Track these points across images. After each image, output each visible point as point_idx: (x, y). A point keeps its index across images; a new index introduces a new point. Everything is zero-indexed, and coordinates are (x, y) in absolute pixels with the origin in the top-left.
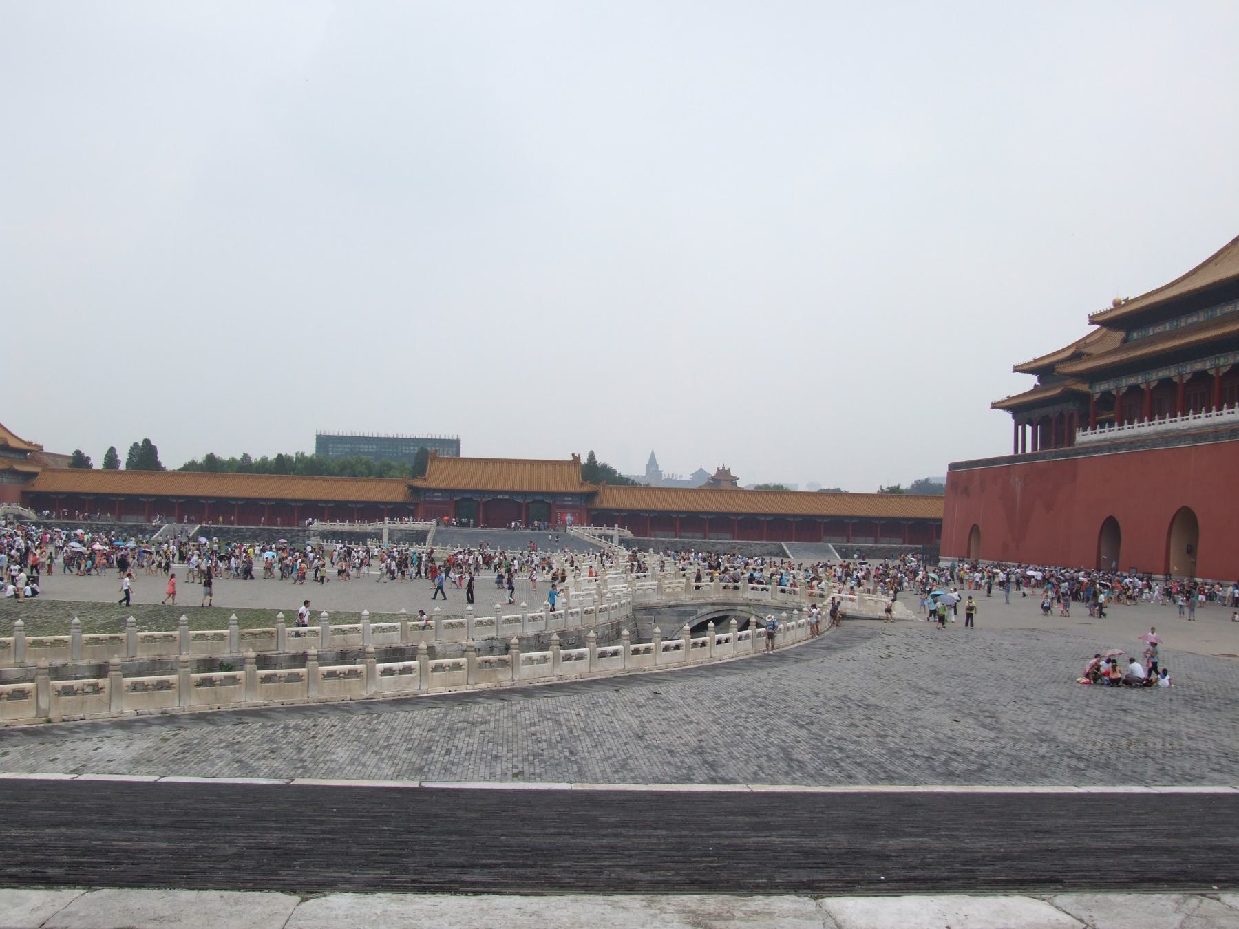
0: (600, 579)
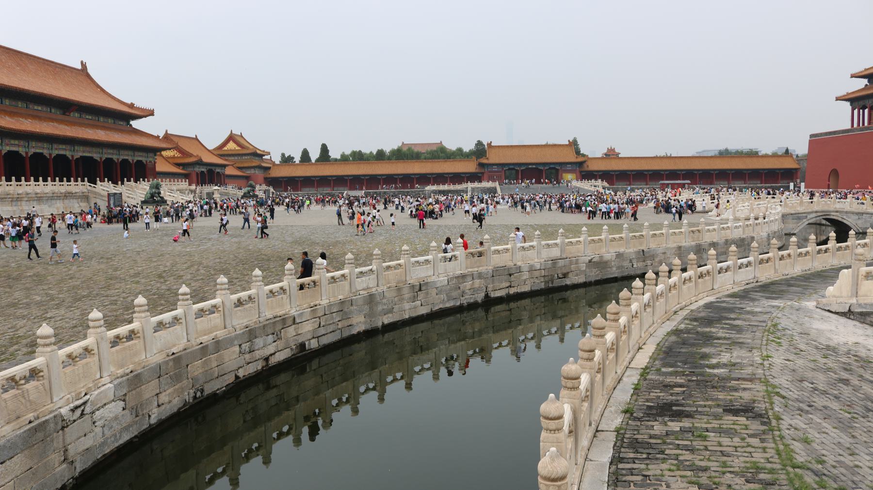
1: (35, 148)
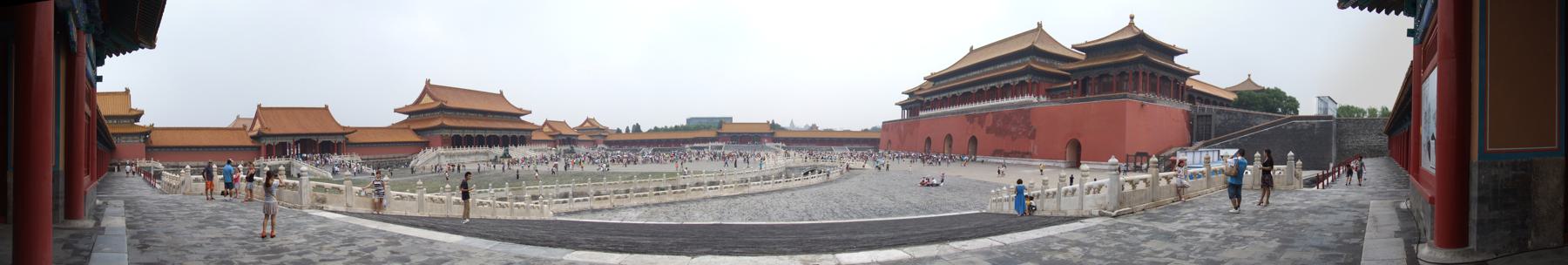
0: (776, 159)
1: (467, 133)
